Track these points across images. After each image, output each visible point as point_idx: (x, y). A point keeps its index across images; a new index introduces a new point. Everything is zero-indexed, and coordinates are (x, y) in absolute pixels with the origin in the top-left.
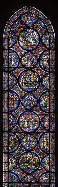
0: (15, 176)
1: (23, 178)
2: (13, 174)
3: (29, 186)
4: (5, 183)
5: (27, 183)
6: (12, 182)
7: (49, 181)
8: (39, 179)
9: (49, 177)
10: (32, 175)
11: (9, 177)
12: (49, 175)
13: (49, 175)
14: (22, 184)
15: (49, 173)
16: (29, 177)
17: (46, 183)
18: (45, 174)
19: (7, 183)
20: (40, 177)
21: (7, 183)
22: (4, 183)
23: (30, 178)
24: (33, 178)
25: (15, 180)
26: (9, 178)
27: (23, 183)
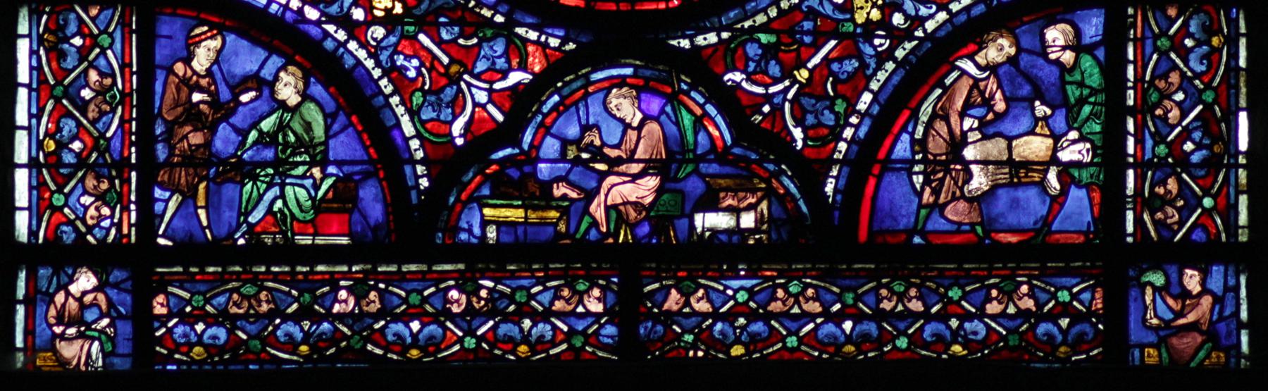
0: (288, 90)
1: (484, 138)
2: (247, 59)
3: (627, 342)
4: (61, 255)
5: (575, 256)
6: (221, 250)
7: (1111, 202)
8: (869, 159)
9: (1114, 114)
10: (703, 70)
11: (147, 116)
12: (1113, 69)
13: (1113, 69)
14: (468, 284)
15: (1093, 26)
16: (625, 106)
17: (1041, 252)
18: (999, 50)
19: (100, 258)
20: (898, 104)
21: (100, 258)
22: (32, 255)
23: (649, 143)
24: (720, 130)
25: (297, 194)
26: (146, 141)
27: (481, 259)
